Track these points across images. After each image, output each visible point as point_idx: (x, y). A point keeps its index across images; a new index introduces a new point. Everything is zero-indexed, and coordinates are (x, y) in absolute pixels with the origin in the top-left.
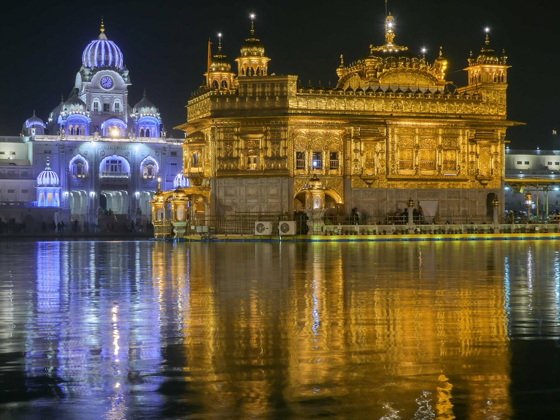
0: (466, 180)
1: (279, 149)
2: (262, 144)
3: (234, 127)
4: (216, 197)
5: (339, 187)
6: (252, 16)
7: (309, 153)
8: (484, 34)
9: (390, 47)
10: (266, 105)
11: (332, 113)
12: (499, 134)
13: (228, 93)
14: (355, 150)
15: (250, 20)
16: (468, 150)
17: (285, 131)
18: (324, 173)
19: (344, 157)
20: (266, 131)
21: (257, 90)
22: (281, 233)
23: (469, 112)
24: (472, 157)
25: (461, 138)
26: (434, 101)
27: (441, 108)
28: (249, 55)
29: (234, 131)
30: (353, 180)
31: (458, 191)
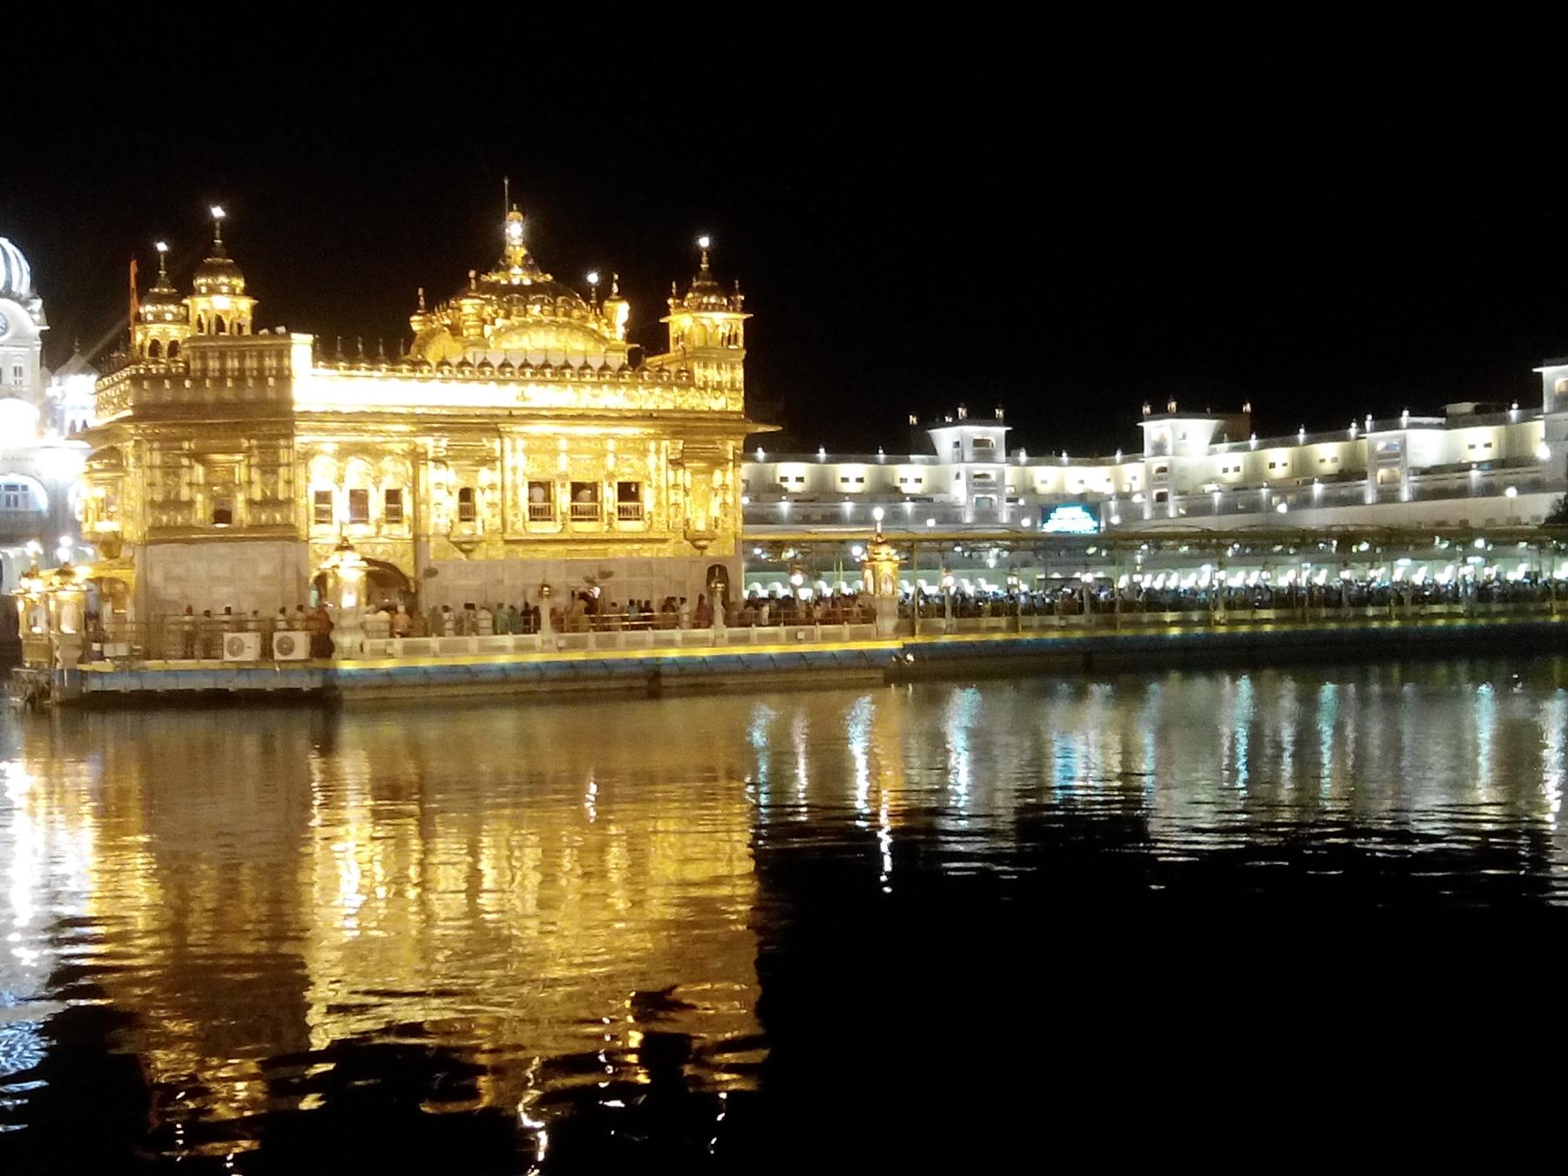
0: (664, 541)
1: (276, 483)
2: (241, 474)
6: (218, 212)
8: (699, 251)
15: (213, 220)
17: (289, 447)
20: (250, 448)
23: (670, 406)
26: (598, 385)
28: (213, 290)
30: (432, 544)
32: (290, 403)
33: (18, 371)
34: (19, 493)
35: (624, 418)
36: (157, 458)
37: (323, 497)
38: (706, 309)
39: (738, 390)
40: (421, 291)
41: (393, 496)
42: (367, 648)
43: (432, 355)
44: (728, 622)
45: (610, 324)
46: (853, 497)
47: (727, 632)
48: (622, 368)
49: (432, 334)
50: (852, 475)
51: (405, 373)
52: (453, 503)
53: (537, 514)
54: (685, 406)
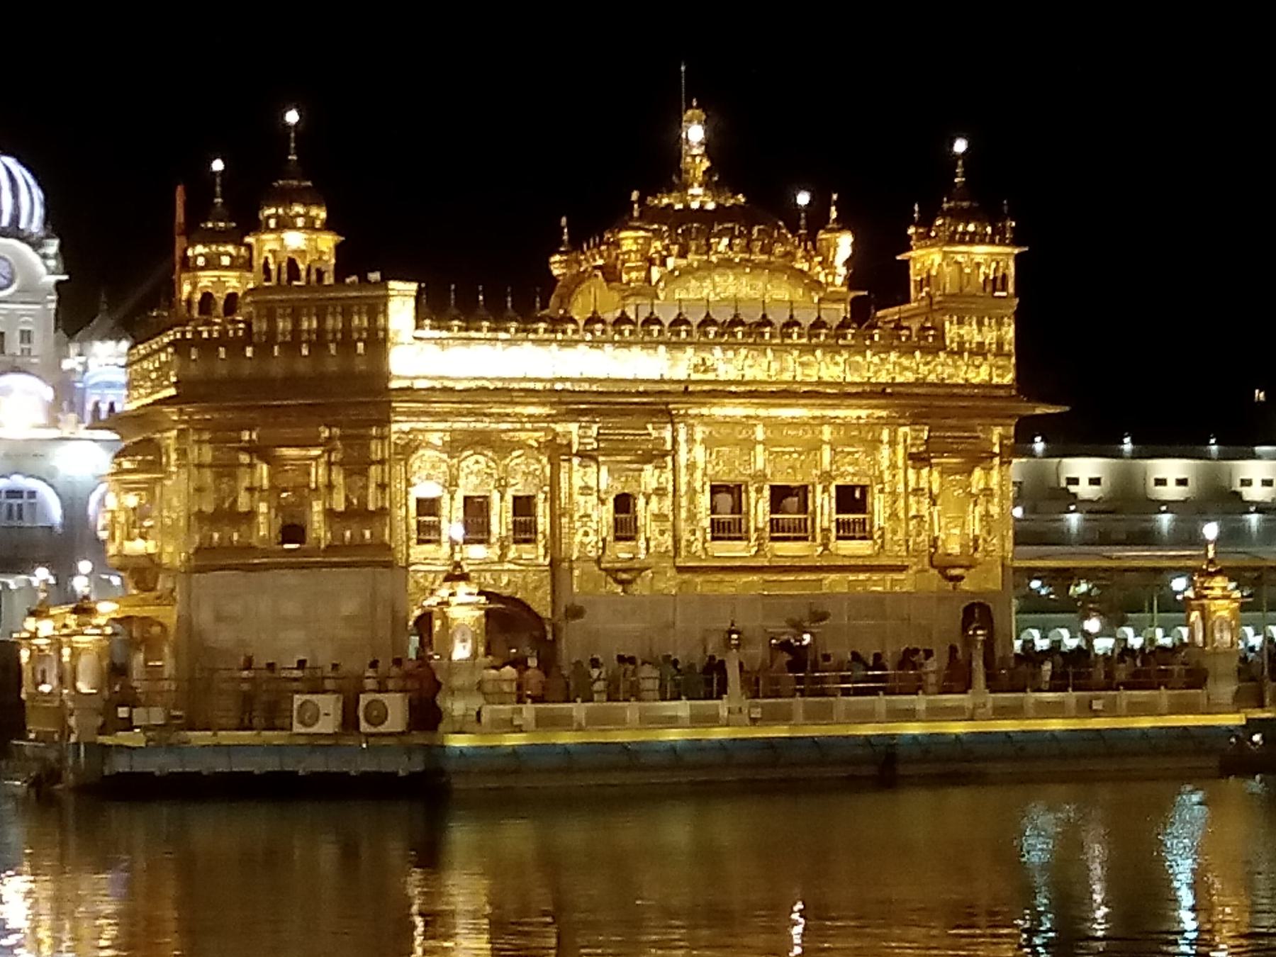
2: (318, 474)
4: (190, 623)
12: (995, 439)
13: (223, 333)
16: (906, 485)
18: (494, 553)
20: (330, 438)
21: (305, 325)
22: (364, 727)
23: (910, 377)
24: (918, 502)
25: (885, 451)
27: (829, 368)
30: (576, 573)
32: (387, 377)
33: (26, 336)
34: (24, 501)
36: (207, 454)
37: (428, 506)
38: (962, 242)
39: (1008, 355)
40: (564, 220)
41: (523, 506)
42: (485, 717)
43: (579, 311)
44: (994, 684)
45: (827, 264)
46: (1171, 506)
47: (992, 698)
48: (844, 325)
49: (579, 279)
50: (1171, 475)
51: (541, 335)
52: (607, 513)
53: (721, 530)
54: (932, 378)
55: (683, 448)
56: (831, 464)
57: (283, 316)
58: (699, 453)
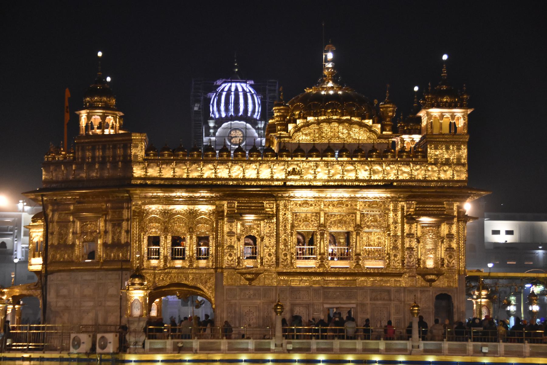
0: (400, 275)
1: (120, 232)
3: (70, 204)
5: (209, 285)
7: (166, 238)
9: (329, 88)
10: (106, 174)
11: (196, 183)
12: (455, 208)
14: (228, 233)
17: (128, 208)
19: (216, 242)
21: (97, 154)
23: (405, 176)
25: (391, 214)
29: (69, 210)
30: (225, 274)
31: (388, 291)
35: (370, 185)
37: (155, 241)
39: (463, 165)
55: (281, 213)
56: (361, 221)
57: (89, 150)
58: (289, 216)
